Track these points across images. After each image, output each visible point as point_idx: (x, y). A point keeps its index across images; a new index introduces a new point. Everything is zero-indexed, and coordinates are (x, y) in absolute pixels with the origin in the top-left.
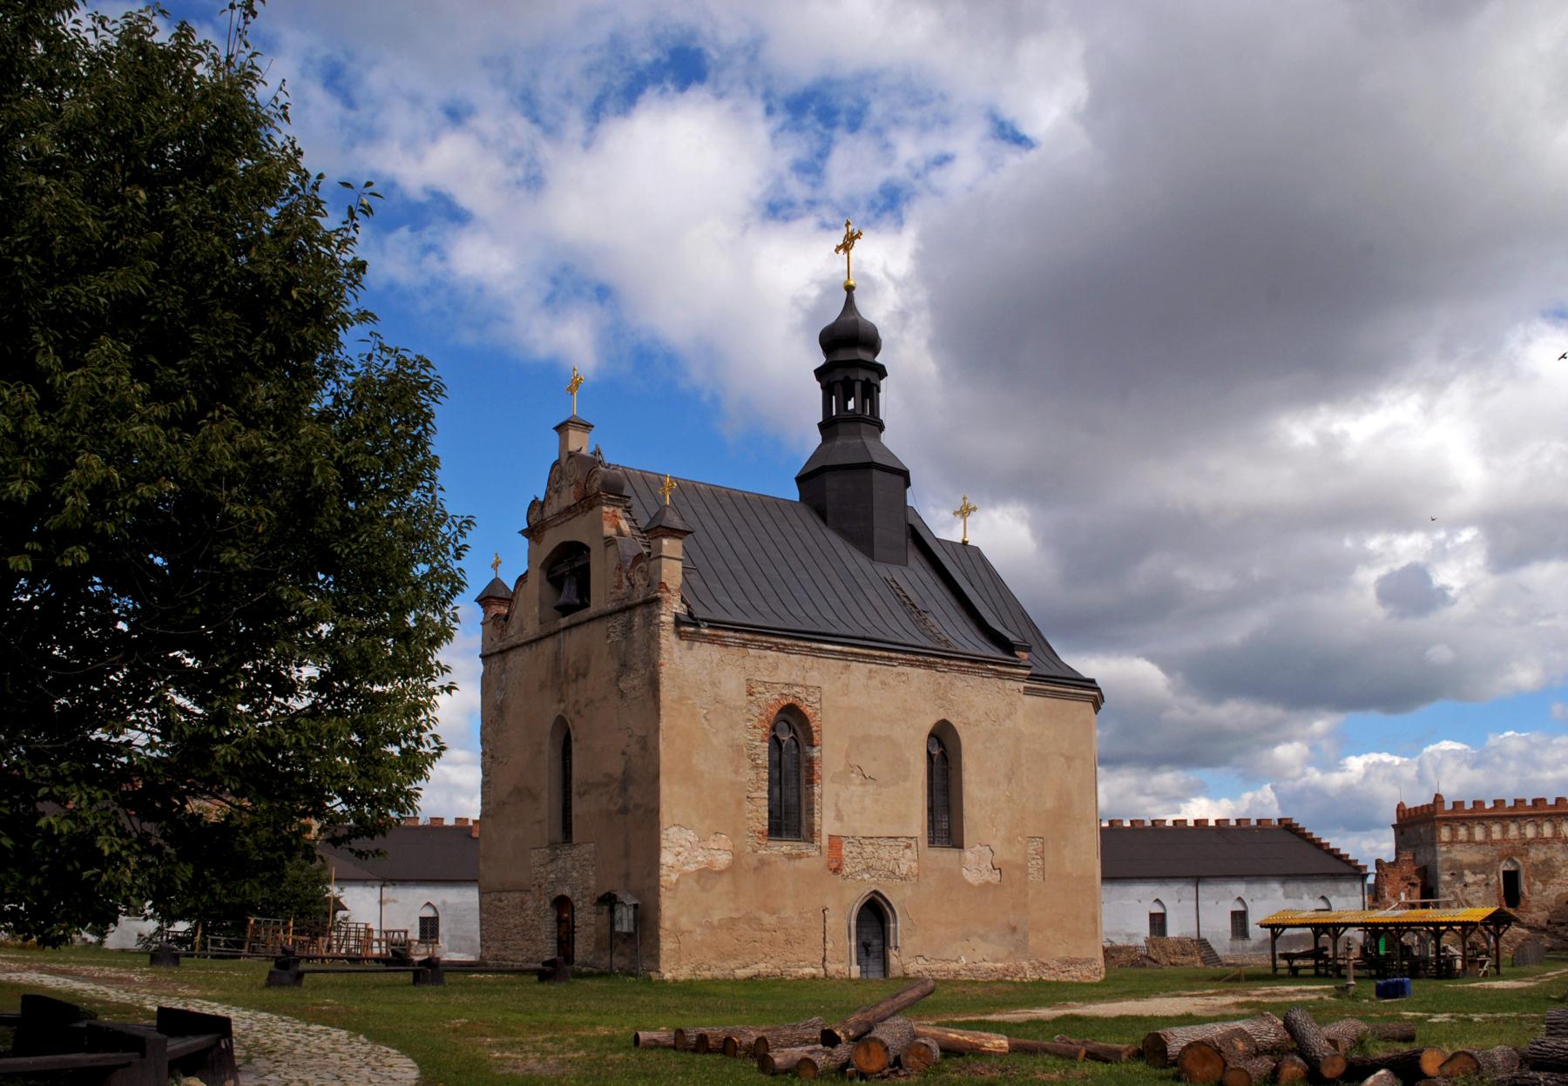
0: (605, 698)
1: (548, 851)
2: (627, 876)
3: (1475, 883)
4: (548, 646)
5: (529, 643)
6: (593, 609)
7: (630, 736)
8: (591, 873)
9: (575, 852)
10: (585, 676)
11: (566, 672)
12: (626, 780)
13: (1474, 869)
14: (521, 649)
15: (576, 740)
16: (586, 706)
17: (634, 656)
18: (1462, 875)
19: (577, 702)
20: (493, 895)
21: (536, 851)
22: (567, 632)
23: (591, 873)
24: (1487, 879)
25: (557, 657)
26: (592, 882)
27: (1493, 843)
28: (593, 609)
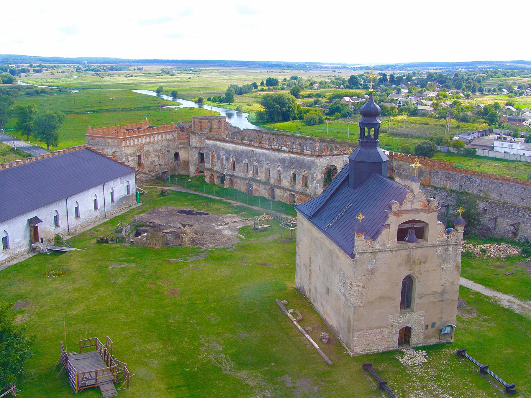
0: (435, 270)
1: (399, 315)
2: (441, 318)
3: (131, 161)
4: (404, 253)
5: (392, 251)
6: (429, 243)
7: (446, 281)
8: (422, 319)
9: (414, 314)
10: (424, 263)
11: (414, 261)
12: (443, 293)
13: (132, 155)
14: (386, 252)
15: (418, 282)
16: (424, 272)
17: (449, 259)
18: (128, 158)
19: (420, 271)
20: (362, 332)
21: (392, 315)
22: (415, 249)
23: (422, 319)
24: (134, 159)
25: (408, 256)
26: (423, 321)
27: (135, 146)
28: (429, 243)
